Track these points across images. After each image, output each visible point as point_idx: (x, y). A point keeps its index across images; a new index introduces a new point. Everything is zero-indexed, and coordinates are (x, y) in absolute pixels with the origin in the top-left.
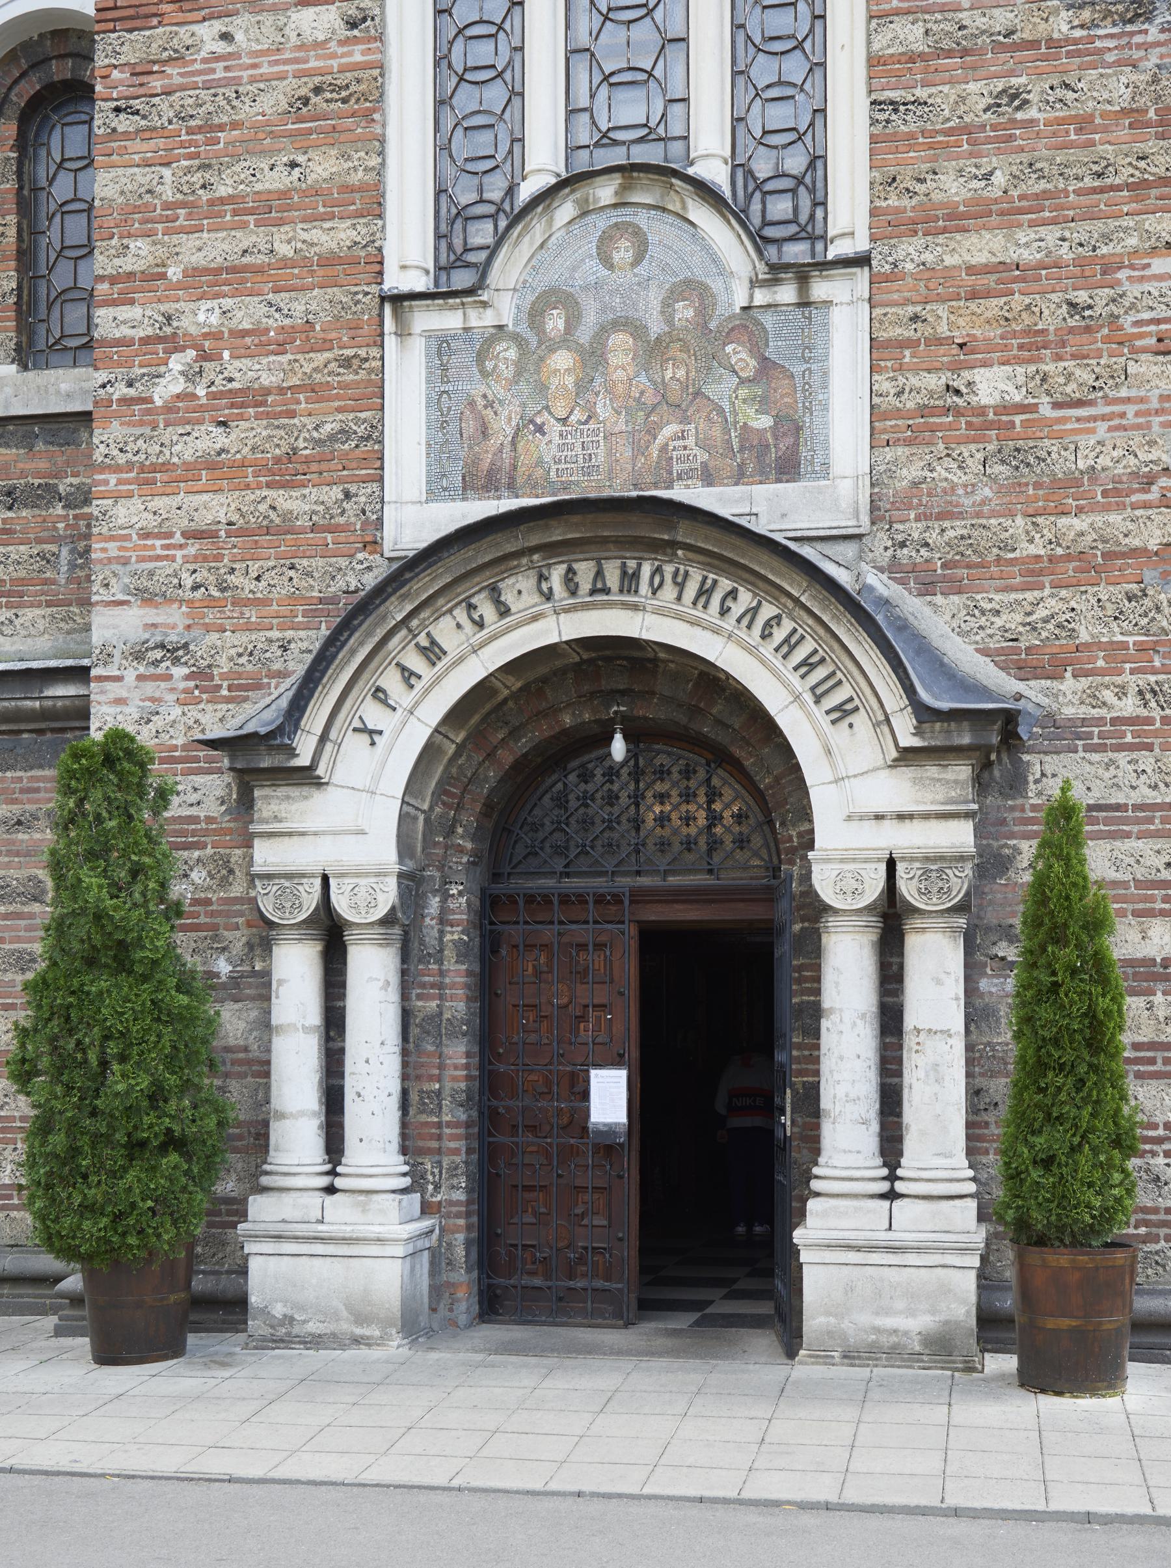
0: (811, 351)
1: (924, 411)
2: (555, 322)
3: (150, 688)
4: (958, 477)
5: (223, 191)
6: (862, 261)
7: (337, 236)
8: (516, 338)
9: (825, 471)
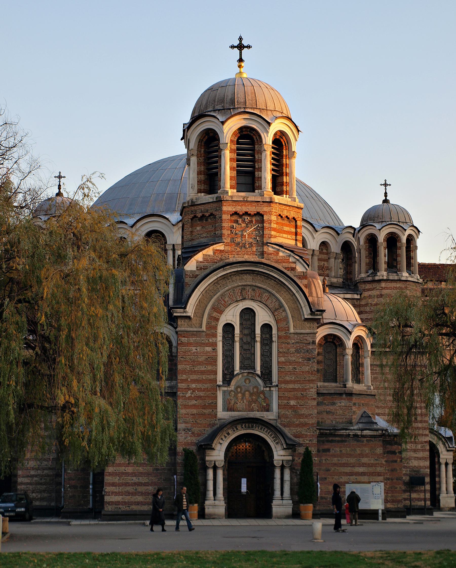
0: (271, 396)
1: (284, 405)
2: (239, 390)
3: (186, 435)
4: (288, 413)
5: (195, 369)
6: (277, 386)
7: (212, 377)
8: (234, 392)
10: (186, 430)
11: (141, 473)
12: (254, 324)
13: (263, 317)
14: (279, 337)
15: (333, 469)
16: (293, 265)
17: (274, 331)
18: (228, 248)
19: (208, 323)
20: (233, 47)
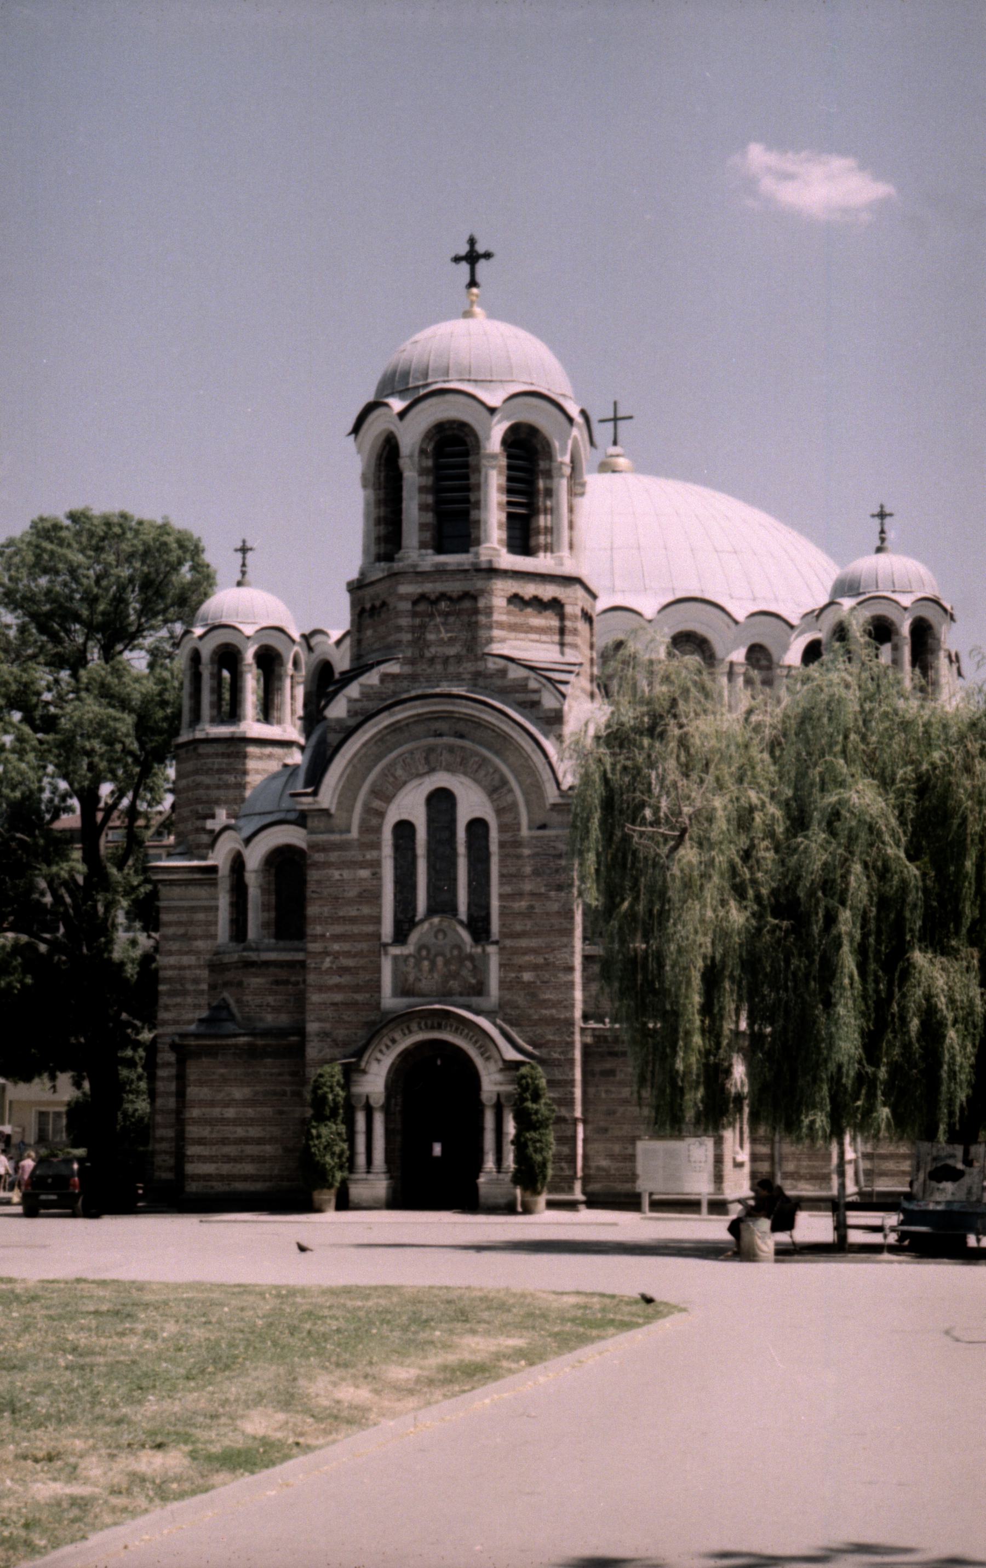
2: (424, 953)
7: (370, 929)
8: (414, 956)
9: (488, 995)
10: (323, 1035)
11: (251, 1119)
12: (453, 821)
13: (471, 803)
14: (502, 845)
15: (621, 1110)
16: (535, 697)
17: (494, 835)
18: (407, 669)
19: (363, 821)
20: (457, 259)
